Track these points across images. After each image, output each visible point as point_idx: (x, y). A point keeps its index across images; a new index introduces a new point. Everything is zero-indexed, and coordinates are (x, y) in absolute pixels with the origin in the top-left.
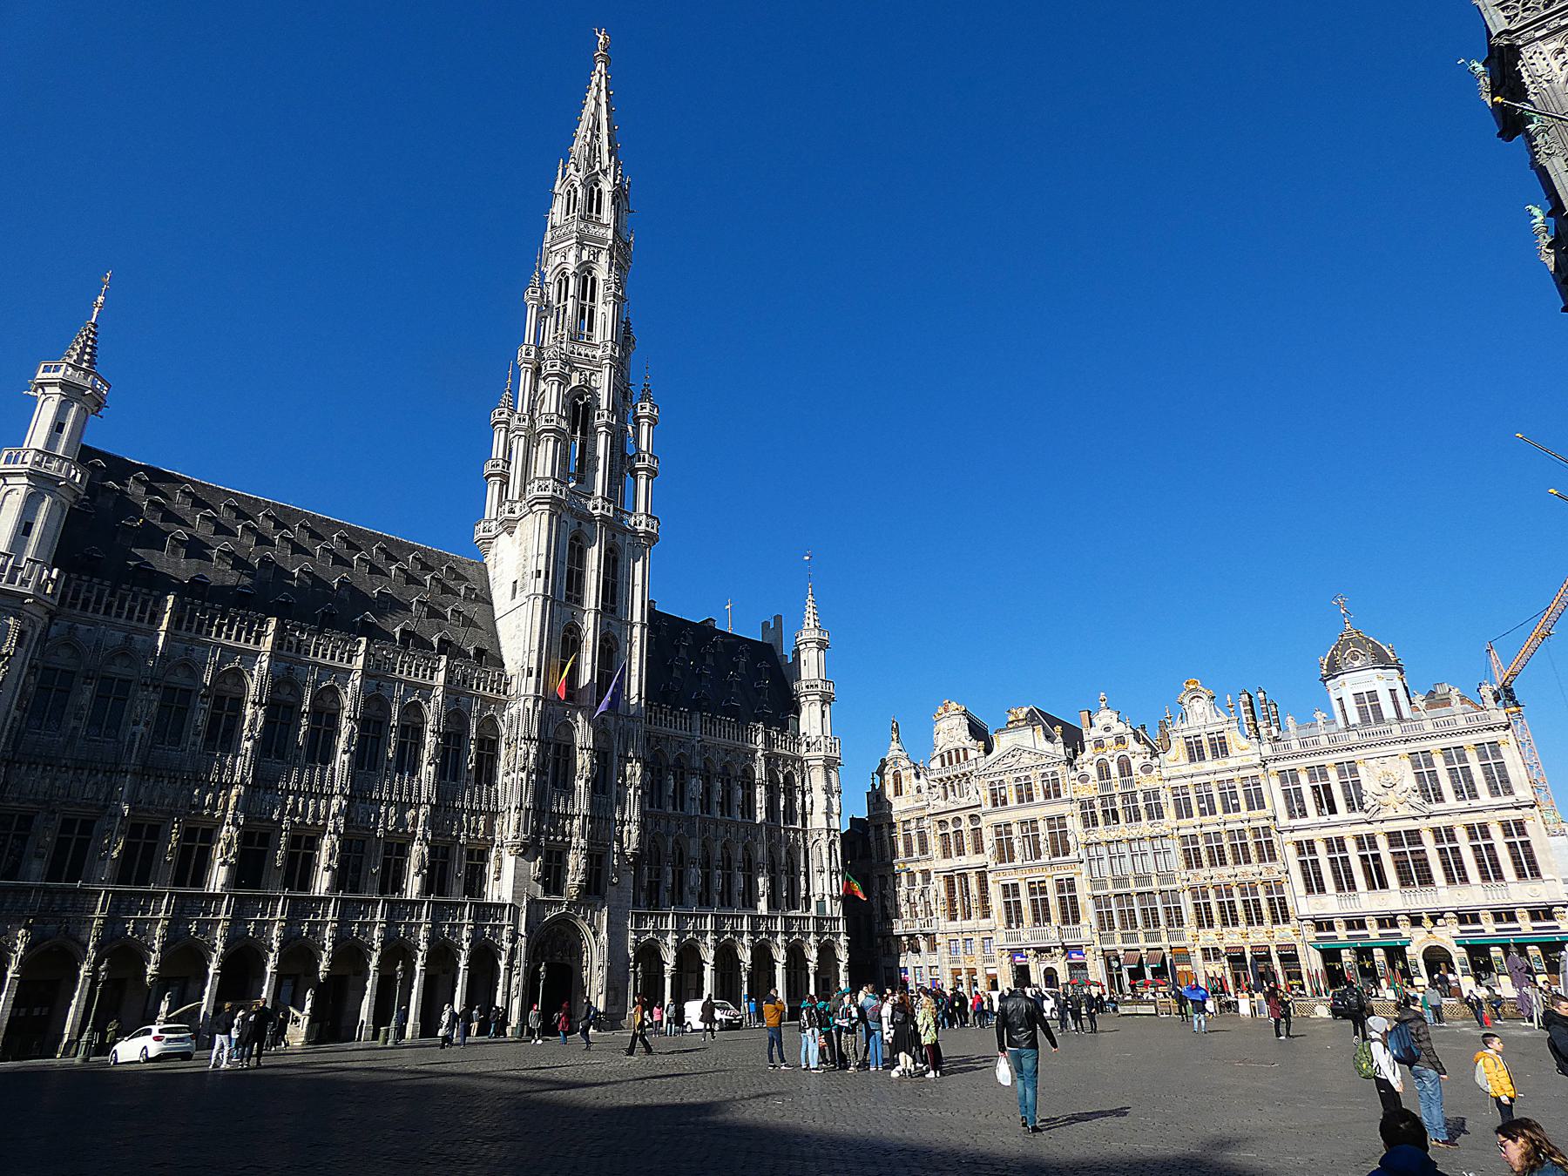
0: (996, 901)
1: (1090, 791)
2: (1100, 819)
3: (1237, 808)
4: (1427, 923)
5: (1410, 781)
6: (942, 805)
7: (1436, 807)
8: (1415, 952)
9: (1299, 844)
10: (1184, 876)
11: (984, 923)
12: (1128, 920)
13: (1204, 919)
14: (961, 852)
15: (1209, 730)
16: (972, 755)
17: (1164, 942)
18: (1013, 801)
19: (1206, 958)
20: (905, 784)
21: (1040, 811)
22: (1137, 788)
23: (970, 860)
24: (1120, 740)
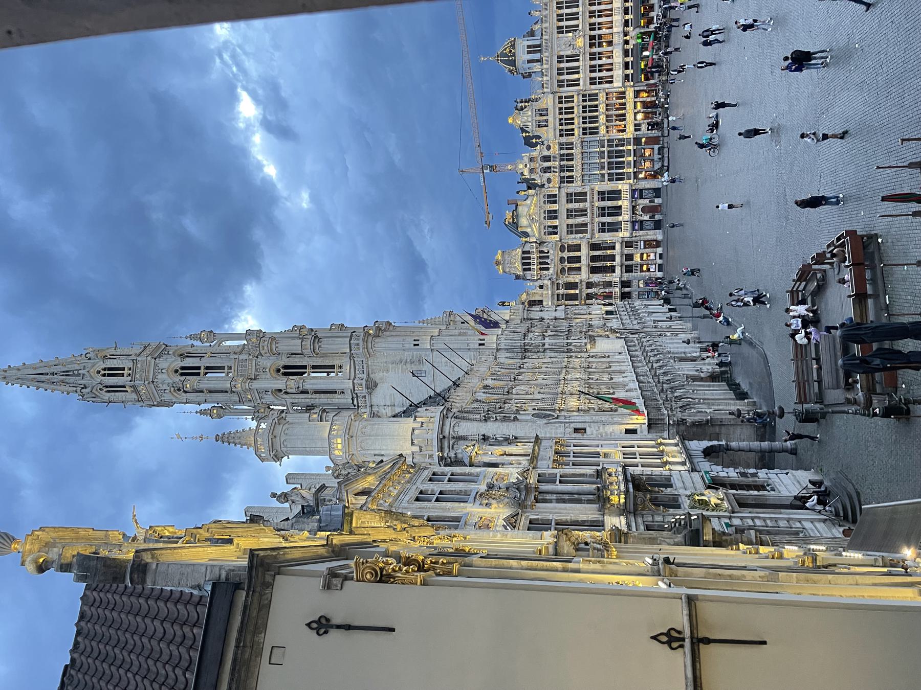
1: (555, 176)
2: (570, 174)
4: (628, 38)
11: (618, 246)
12: (620, 165)
17: (631, 147)
19: (639, 130)
20: (538, 298)
21: (562, 206)
23: (584, 253)
24: (532, 160)
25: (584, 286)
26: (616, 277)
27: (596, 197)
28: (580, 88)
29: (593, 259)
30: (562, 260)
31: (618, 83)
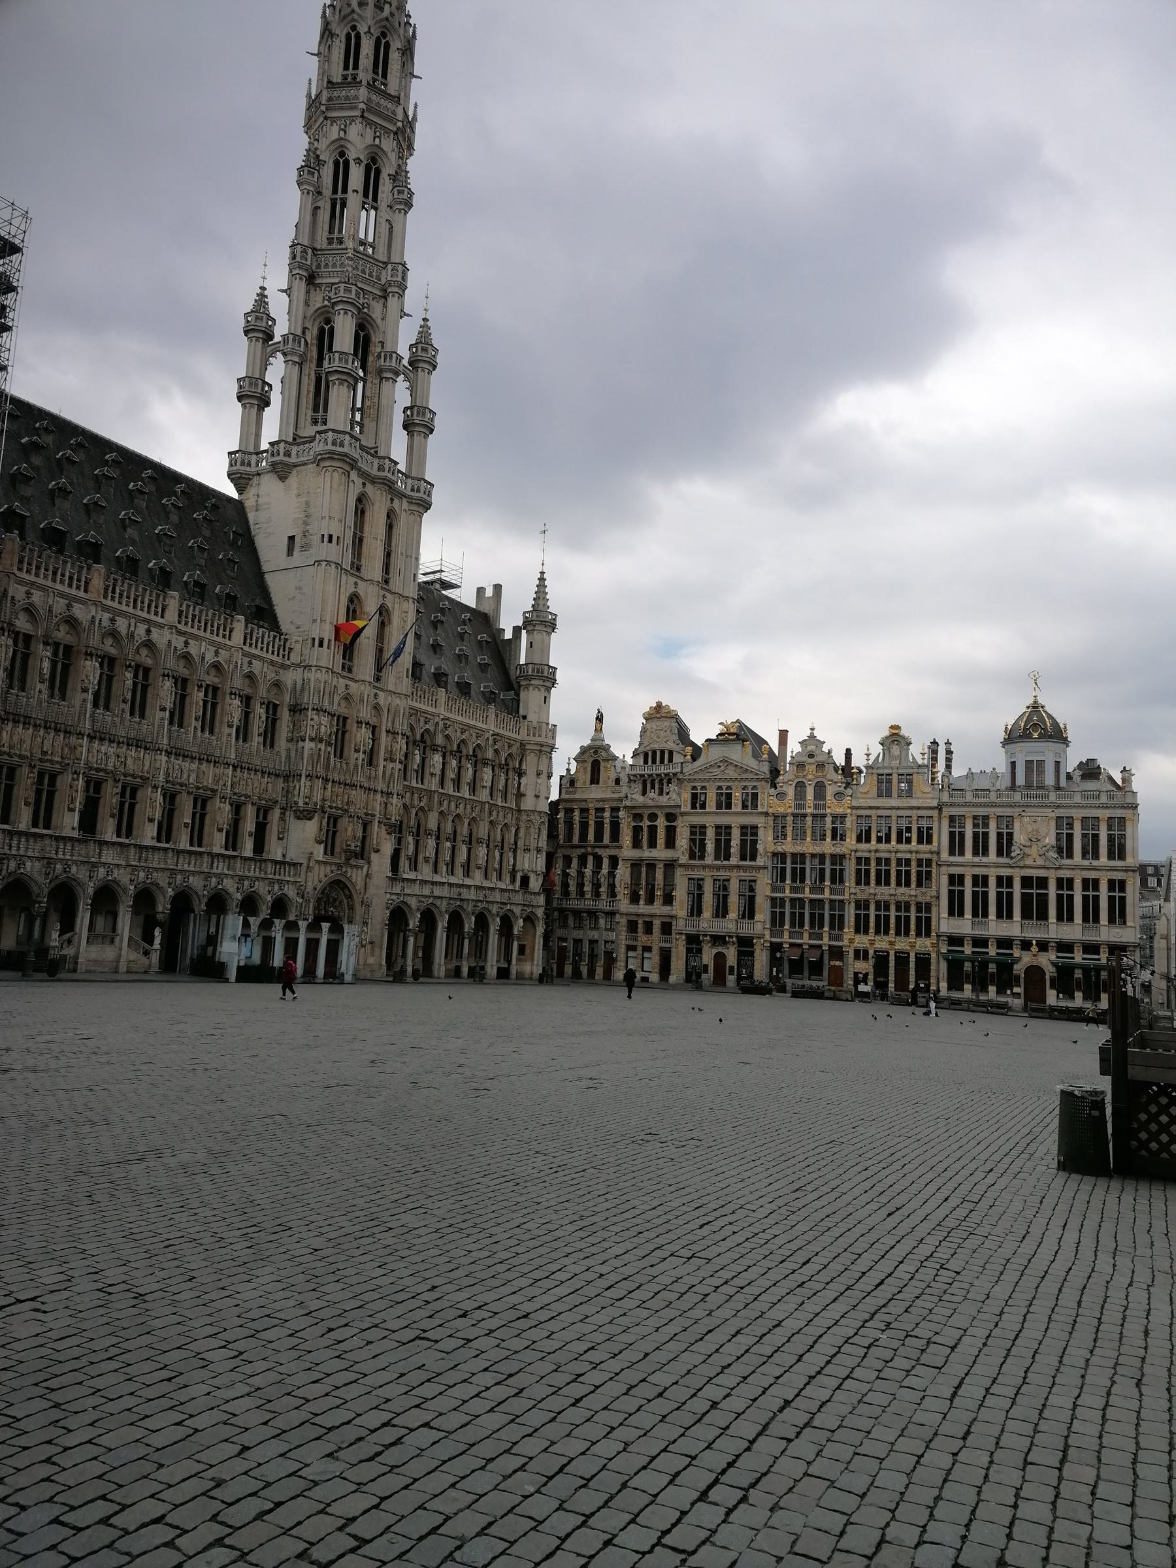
0: (681, 893)
1: (786, 807)
3: (909, 841)
4: (1034, 949)
5: (1050, 840)
6: (640, 799)
7: (1066, 862)
8: (1019, 969)
9: (951, 877)
10: (852, 890)
11: (666, 910)
13: (861, 926)
14: (652, 844)
15: (901, 771)
16: (677, 758)
18: (711, 806)
21: (736, 819)
22: (828, 811)
23: (660, 853)
25: (613, 852)
26: (624, 905)
27: (746, 875)
28: (945, 856)
29: (651, 866)
30: (652, 817)
31: (945, 924)
